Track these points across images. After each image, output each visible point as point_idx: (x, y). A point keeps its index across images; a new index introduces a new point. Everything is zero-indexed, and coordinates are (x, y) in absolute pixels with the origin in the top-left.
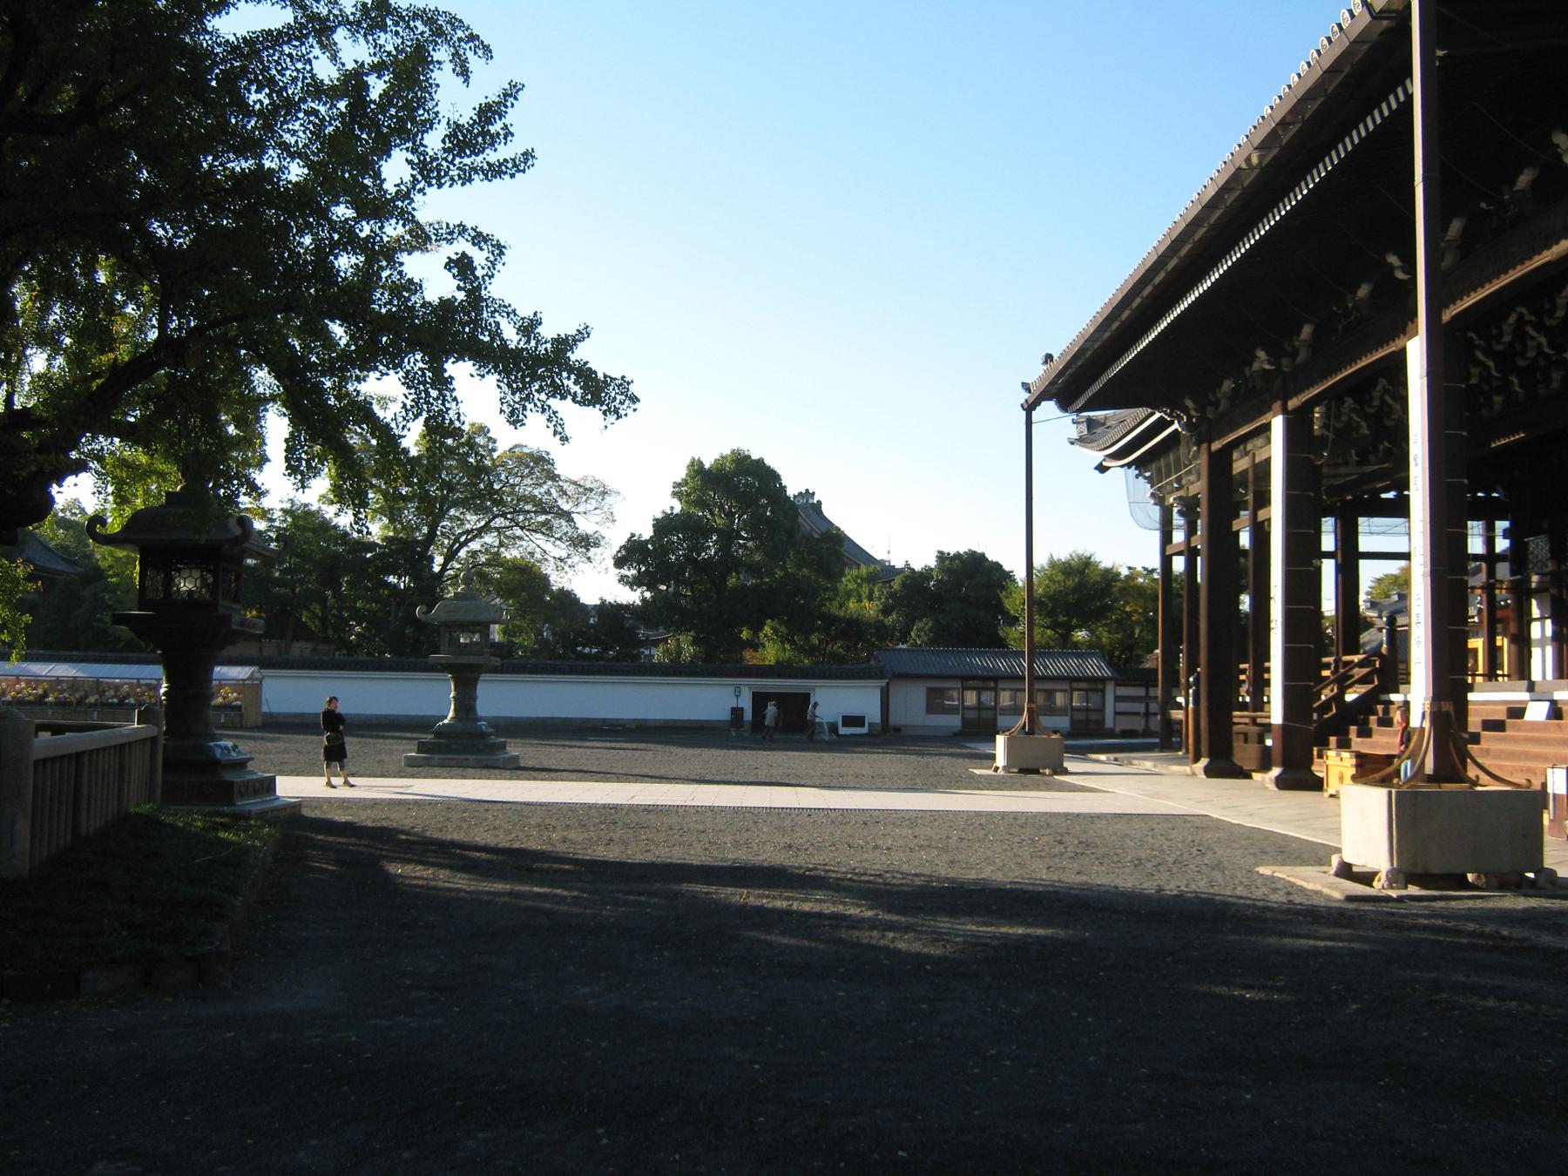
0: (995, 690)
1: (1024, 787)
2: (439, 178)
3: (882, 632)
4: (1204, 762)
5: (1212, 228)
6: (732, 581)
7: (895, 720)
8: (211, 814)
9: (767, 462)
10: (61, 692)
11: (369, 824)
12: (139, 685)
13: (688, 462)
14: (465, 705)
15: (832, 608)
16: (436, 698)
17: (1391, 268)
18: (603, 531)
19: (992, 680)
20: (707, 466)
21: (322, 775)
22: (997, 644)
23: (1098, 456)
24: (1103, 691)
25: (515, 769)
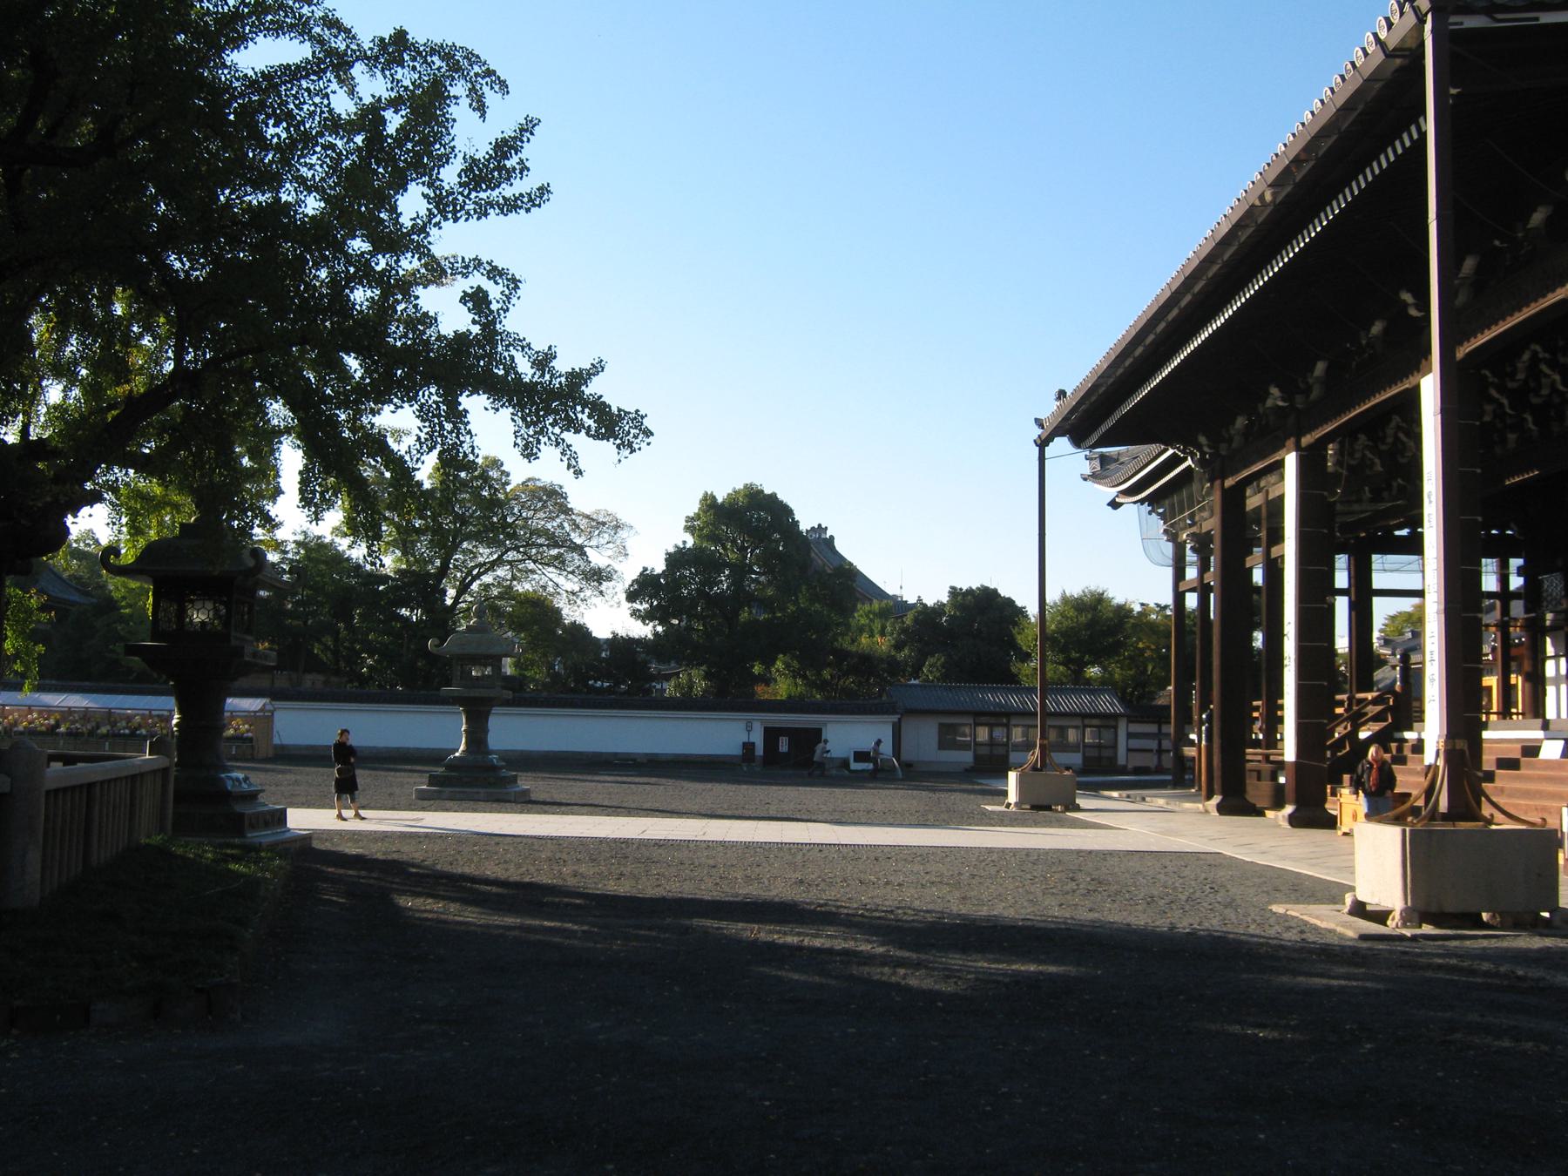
0: (1007, 726)
1: (1036, 824)
2: (455, 212)
3: (894, 667)
4: (1217, 799)
5: (1225, 265)
6: (744, 616)
8: (221, 846)
10: (73, 722)
11: (380, 856)
12: (151, 716)
13: (701, 496)
14: (477, 737)
15: (845, 643)
16: (446, 731)
17: (1405, 305)
19: (1003, 717)
20: (720, 500)
21: (333, 807)
22: (1009, 680)
23: (1112, 492)
24: (1116, 728)
25: (526, 803)
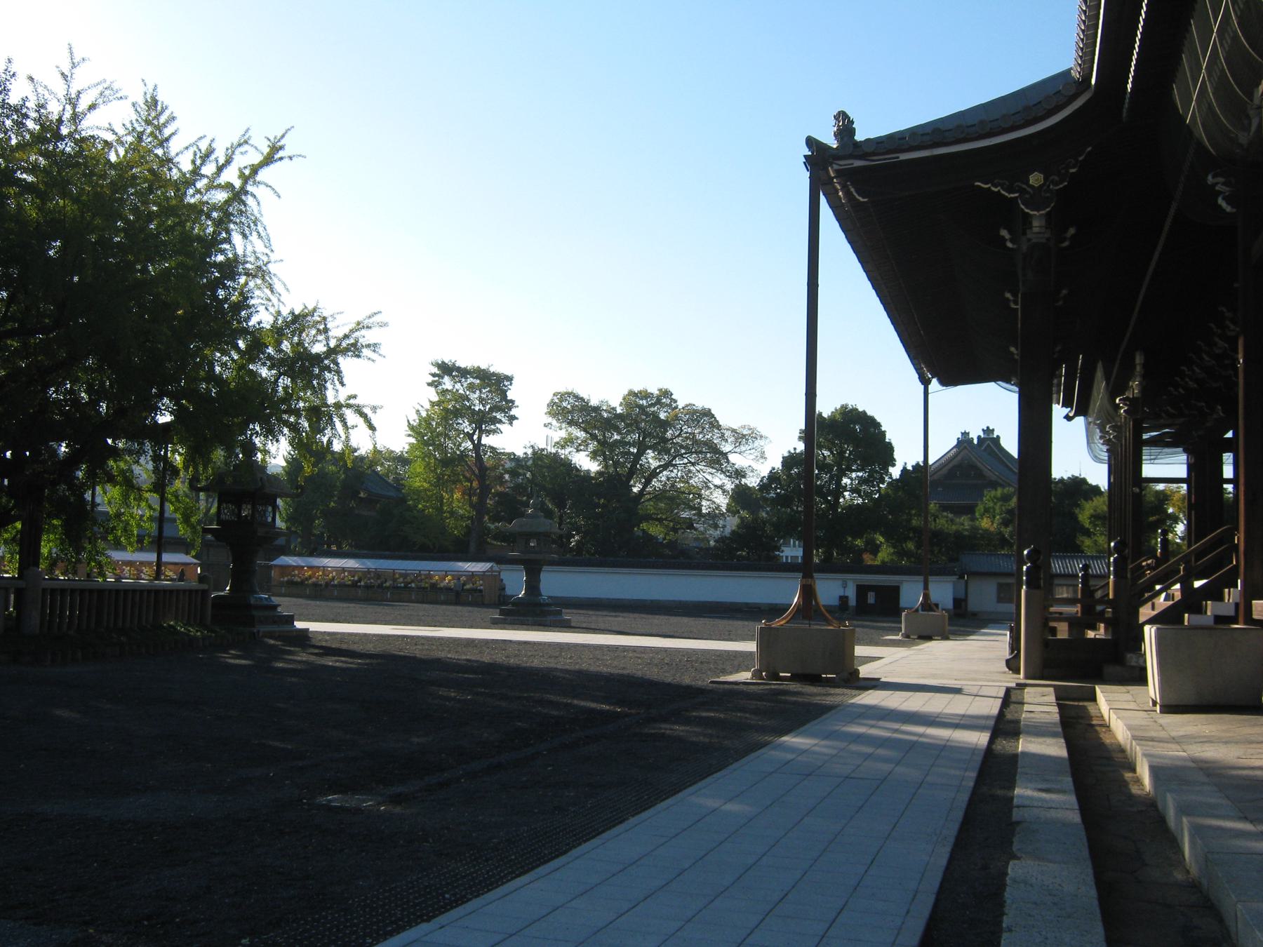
3: (1004, 542)
7: (973, 605)
9: (869, 413)
14: (533, 586)
18: (755, 466)
20: (825, 415)
25: (566, 626)
